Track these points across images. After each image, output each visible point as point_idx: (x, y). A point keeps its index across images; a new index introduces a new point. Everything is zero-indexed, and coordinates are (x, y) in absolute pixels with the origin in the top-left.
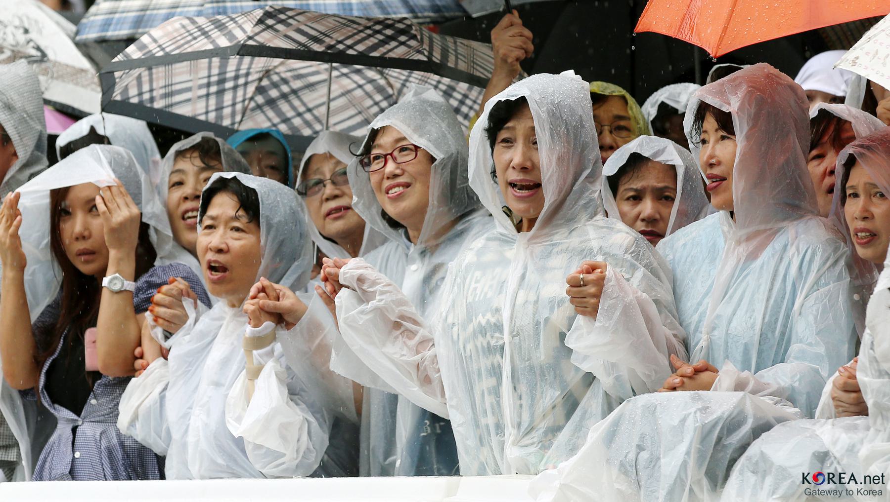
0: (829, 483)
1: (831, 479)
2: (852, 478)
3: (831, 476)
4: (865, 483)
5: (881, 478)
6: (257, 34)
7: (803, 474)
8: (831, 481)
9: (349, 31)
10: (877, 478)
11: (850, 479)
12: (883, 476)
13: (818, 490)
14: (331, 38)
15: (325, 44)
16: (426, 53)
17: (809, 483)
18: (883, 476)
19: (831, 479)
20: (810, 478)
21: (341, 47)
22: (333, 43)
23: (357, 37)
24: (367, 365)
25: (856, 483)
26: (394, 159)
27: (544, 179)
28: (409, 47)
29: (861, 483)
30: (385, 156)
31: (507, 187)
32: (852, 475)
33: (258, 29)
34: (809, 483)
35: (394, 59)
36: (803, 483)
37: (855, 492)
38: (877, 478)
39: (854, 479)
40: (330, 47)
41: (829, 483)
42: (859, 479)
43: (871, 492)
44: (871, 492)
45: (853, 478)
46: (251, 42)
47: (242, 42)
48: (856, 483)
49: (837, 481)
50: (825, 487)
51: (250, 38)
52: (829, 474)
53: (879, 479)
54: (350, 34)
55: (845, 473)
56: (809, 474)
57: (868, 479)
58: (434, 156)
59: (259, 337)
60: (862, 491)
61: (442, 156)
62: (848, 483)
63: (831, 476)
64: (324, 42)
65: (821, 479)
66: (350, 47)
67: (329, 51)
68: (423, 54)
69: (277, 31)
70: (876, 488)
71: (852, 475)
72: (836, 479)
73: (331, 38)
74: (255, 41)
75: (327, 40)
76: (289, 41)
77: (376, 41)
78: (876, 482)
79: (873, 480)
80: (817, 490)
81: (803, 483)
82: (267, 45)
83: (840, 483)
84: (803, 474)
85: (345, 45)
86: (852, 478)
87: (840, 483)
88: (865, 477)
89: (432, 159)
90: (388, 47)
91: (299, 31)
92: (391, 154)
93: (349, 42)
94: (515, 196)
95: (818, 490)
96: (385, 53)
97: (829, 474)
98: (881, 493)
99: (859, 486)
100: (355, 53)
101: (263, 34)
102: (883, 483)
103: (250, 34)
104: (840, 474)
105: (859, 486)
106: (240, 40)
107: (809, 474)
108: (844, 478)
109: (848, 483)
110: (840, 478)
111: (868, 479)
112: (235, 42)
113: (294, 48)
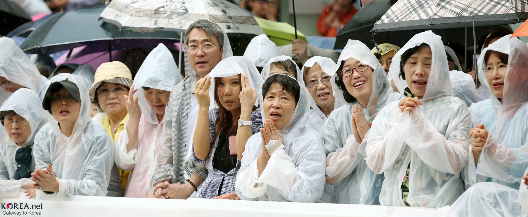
0: (15, 208)
1: (16, 206)
2: (26, 206)
3: (16, 205)
4: (33, 209)
5: (40, 206)
6: (438, 12)
7: (2, 204)
8: (15, 207)
9: (479, 2)
10: (39, 206)
11: (25, 207)
12: (41, 205)
13: (9, 212)
14: (471, 8)
15: (469, 12)
16: (514, 9)
17: (5, 208)
18: (41, 205)
19: (16, 206)
20: (5, 206)
21: (476, 12)
22: (472, 10)
23: (483, 5)
24: (382, 189)
25: (28, 208)
26: (357, 71)
27: (430, 76)
28: (507, 7)
29: (31, 209)
30: (353, 69)
31: (411, 83)
32: (26, 204)
33: (438, 9)
34: (5, 208)
35: (500, 14)
36: (2, 208)
37: (28, 213)
38: (39, 206)
39: (27, 207)
40: (471, 13)
41: (15, 208)
42: (30, 206)
43: (36, 213)
44: (36, 213)
45: (26, 206)
46: (436, 17)
47: (432, 17)
48: (28, 208)
49: (19, 208)
50: (13, 210)
51: (435, 14)
52: (15, 204)
53: (40, 207)
54: (479, 4)
55: (23, 204)
56: (5, 204)
57: (34, 206)
58: (374, 69)
59: (208, 170)
60: (31, 213)
61: (376, 68)
62: (24, 208)
63: (16, 205)
64: (468, 10)
65: (10, 206)
66: (480, 11)
67: (471, 15)
68: (513, 10)
69: (447, 8)
70: (39, 211)
71: (26, 204)
72: (18, 207)
73: (471, 8)
74: (438, 16)
75: (469, 9)
76: (453, 13)
77: (491, 6)
78: (38, 208)
79: (37, 207)
80: (9, 212)
81: (2, 208)
82: (443, 17)
83: (20, 208)
84: (2, 204)
85: (477, 10)
86: (26, 206)
87: (20, 208)
88: (33, 206)
89: (373, 70)
90: (497, 8)
91: (456, 6)
92: (355, 68)
93: (479, 9)
94: (416, 87)
95: (9, 212)
96: (496, 12)
97: (15, 204)
98: (40, 213)
99: (30, 210)
100: (482, 14)
101: (440, 11)
102: (42, 209)
103: (435, 12)
104: (20, 204)
105: (30, 210)
106: (431, 16)
107: (5, 204)
108: (22, 206)
109: (24, 208)
110: (20, 206)
111: (34, 206)
112: (429, 16)
113: (455, 16)
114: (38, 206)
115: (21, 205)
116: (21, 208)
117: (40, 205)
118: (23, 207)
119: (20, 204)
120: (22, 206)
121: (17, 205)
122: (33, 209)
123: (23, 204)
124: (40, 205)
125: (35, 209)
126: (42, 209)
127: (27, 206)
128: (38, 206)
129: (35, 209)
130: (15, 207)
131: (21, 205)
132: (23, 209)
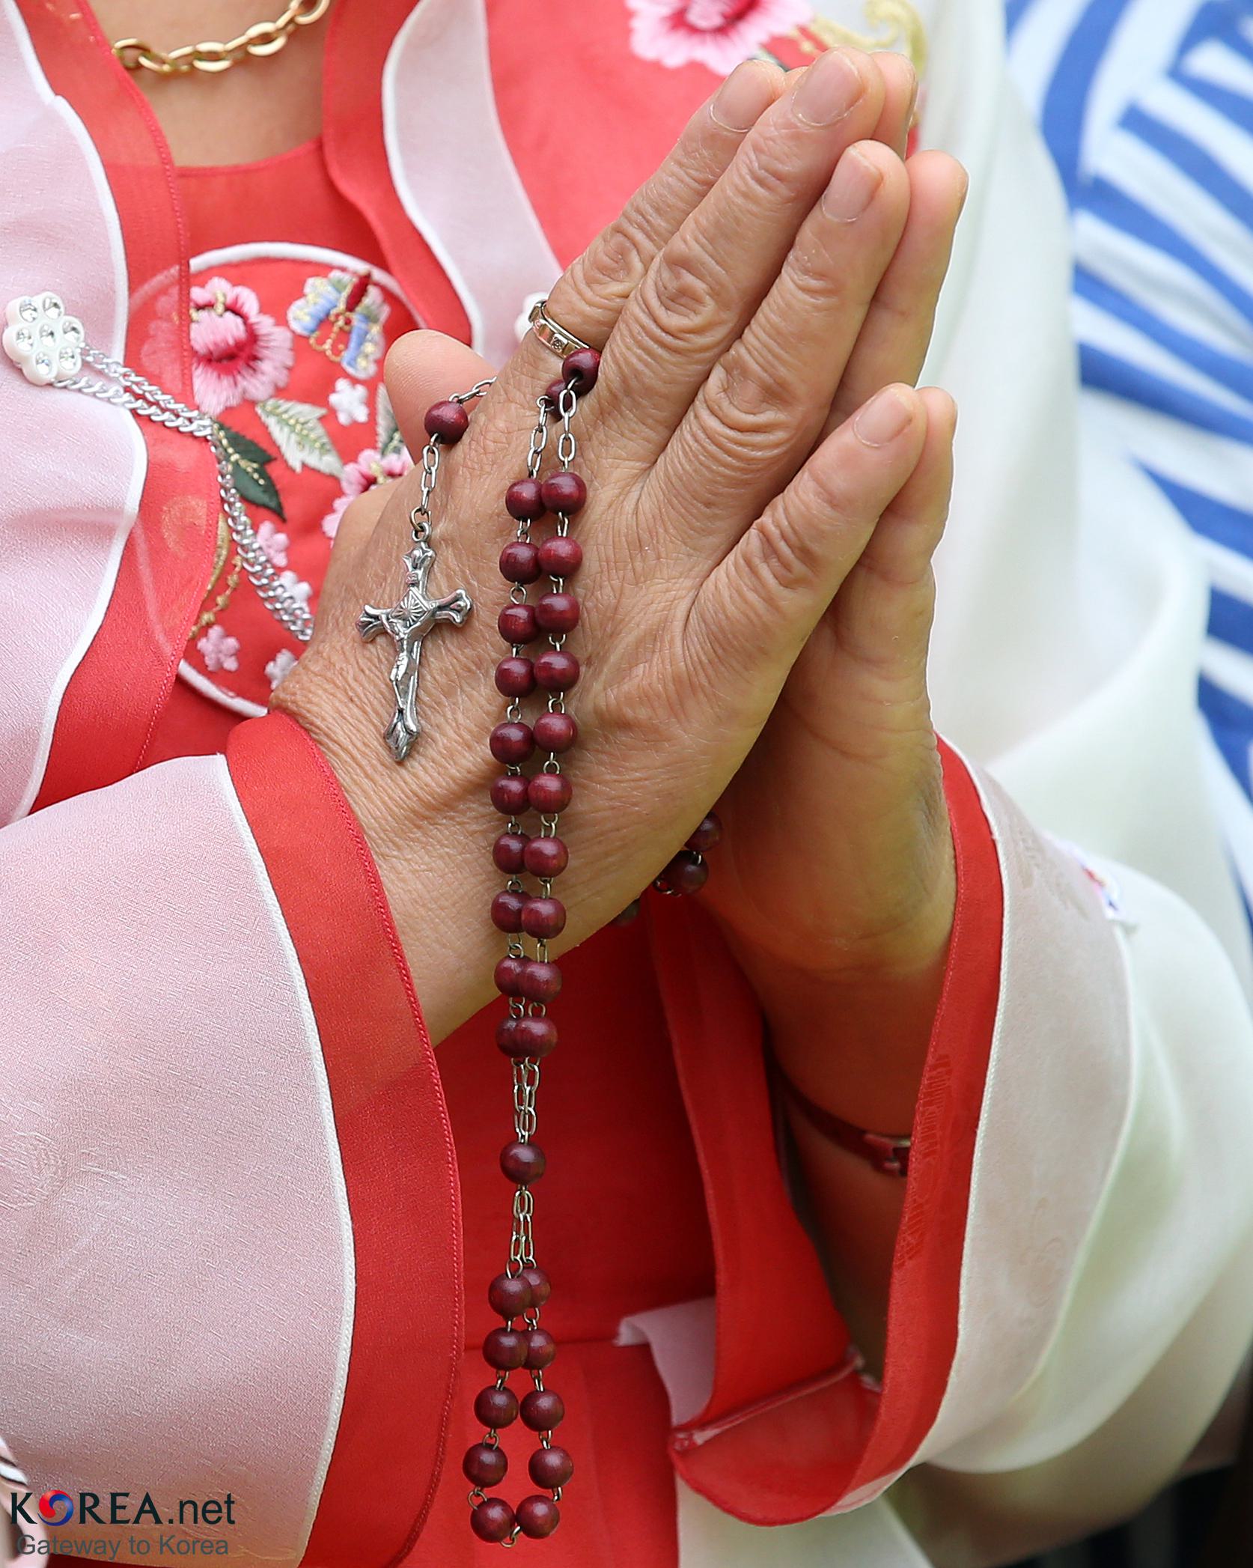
0: (83, 1520)
1: (90, 1509)
2: (147, 1507)
3: (89, 1501)
4: (181, 1521)
5: (225, 1510)
8: (88, 1516)
11: (142, 1511)
18: (229, 1502)
25: (158, 1521)
29: (171, 1521)
32: (147, 1499)
39: (153, 1511)
41: (83, 1520)
42: (167, 1509)
48: (158, 1521)
52: (83, 1496)
53: (220, 1511)
55: (127, 1495)
57: (189, 1510)
62: (137, 1521)
63: (89, 1501)
65: (60, 1507)
71: (147, 1499)
72: (104, 1510)
78: (212, 1517)
79: (204, 1511)
86: (147, 1507)
87: (114, 1520)
88: (182, 1505)
97: (83, 1496)
102: (231, 1522)
104: (114, 1496)
108: (124, 1507)
109: (137, 1521)
110: (114, 1507)
111: (189, 1510)
114: (210, 1507)
115: (120, 1501)
116: (118, 1519)
118: (131, 1513)
119: (114, 1496)
120: (124, 1507)
121: (97, 1502)
122: (181, 1521)
123: (127, 1495)
125: (196, 1521)
126: (231, 1522)
128: (210, 1507)
129: (196, 1521)
130: (88, 1516)
132: (127, 1522)
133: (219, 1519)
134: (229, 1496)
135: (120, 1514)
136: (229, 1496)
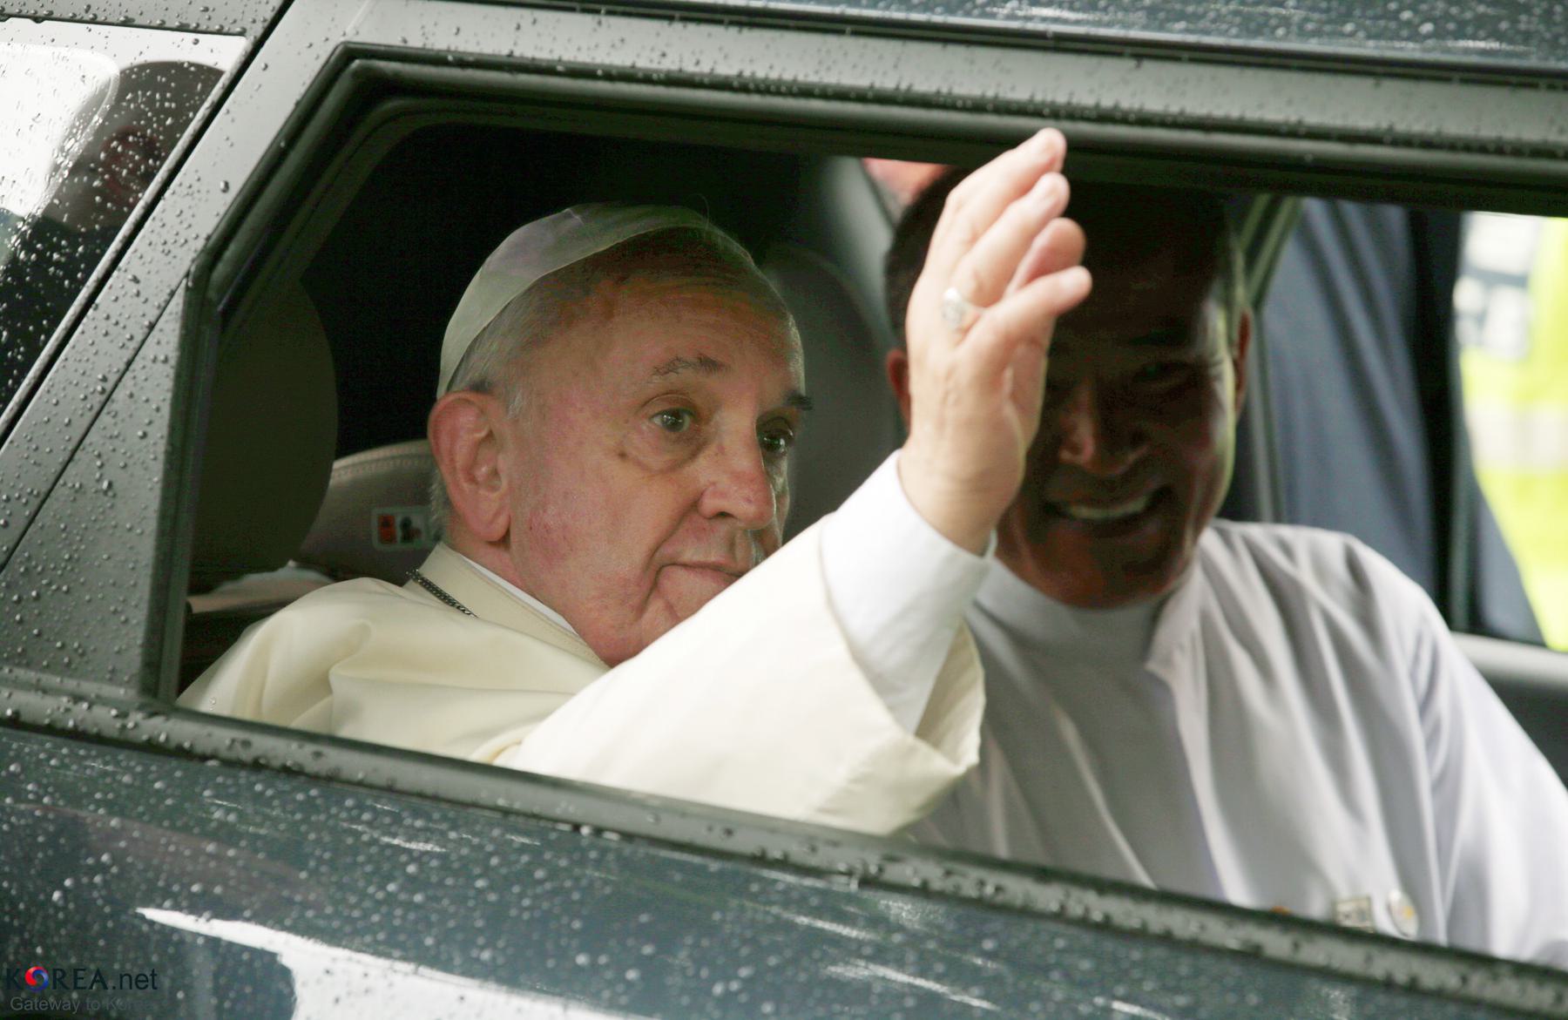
1: (59, 980)
2: (98, 978)
3: (59, 974)
5: (150, 978)
10: (144, 979)
12: (153, 975)
38: (144, 979)
53: (147, 981)
57: (126, 979)
63: (59, 974)
78: (142, 985)
79: (137, 981)
88: (122, 977)
104: (76, 971)
110: (76, 979)
111: (126, 979)
117: (148, 973)
124: (148, 973)
125: (131, 988)
127: (101, 977)
129: (131, 988)
131: (81, 974)
132: (85, 988)
133: (147, 986)
134: (153, 971)
135: (80, 983)
136: (153, 971)
